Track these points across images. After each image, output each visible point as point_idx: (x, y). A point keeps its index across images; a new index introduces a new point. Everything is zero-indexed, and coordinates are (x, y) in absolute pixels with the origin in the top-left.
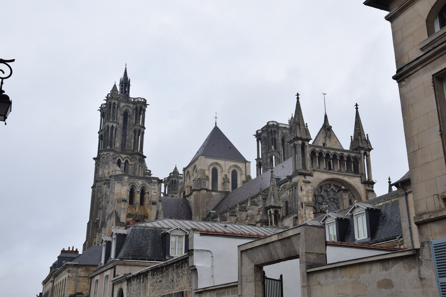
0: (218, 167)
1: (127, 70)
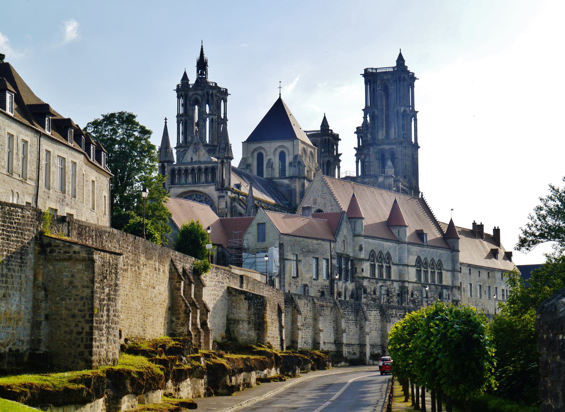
0: (263, 151)
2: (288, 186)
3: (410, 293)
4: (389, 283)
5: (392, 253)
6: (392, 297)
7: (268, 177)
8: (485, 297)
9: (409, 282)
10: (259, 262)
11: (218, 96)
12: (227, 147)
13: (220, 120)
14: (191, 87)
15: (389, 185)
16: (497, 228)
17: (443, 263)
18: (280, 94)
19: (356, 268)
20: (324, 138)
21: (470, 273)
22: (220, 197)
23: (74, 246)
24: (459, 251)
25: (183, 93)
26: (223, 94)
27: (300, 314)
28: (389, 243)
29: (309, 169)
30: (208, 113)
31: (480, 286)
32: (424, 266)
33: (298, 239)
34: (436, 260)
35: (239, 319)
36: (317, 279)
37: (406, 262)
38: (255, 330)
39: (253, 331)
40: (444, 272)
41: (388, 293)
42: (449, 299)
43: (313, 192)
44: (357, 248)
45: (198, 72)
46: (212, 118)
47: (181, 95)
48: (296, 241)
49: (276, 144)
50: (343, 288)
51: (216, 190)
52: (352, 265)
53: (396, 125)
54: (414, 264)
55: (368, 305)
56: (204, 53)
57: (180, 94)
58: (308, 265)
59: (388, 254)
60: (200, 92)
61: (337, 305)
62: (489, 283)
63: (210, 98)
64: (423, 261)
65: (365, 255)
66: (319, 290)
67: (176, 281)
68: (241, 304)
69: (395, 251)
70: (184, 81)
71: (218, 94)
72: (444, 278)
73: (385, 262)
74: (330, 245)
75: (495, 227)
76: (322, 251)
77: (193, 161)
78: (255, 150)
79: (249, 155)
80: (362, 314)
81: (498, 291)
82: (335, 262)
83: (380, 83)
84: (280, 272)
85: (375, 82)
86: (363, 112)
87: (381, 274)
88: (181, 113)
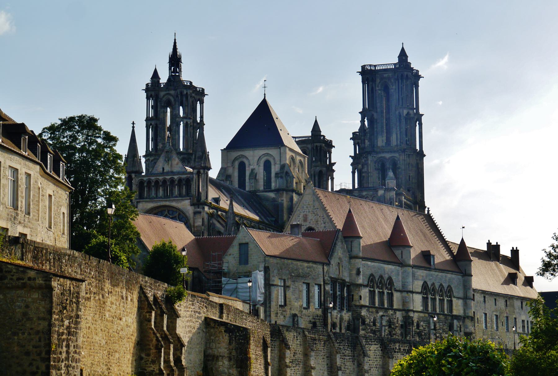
1: (177, 41)
2: (274, 200)
3: (415, 324)
4: (391, 312)
5: (394, 278)
6: (394, 329)
7: (252, 189)
8: (502, 329)
9: (414, 312)
10: (240, 289)
11: (194, 97)
12: (204, 155)
13: (195, 124)
14: (162, 86)
15: (390, 199)
16: (515, 249)
17: (453, 289)
18: (265, 95)
19: (353, 295)
20: (315, 144)
21: (485, 301)
22: (195, 213)
23: (29, 271)
24: (472, 276)
25: (153, 93)
26: (200, 94)
27: (289, 348)
28: (390, 266)
29: (298, 181)
30: (182, 116)
31: (497, 316)
32: (431, 293)
33: (286, 261)
34: (445, 285)
35: (218, 354)
36: (308, 308)
37: (410, 288)
38: (237, 367)
39: (235, 369)
40: (454, 300)
41: (390, 324)
42: (461, 331)
43: (303, 207)
44: (354, 272)
45: (170, 69)
46: (187, 122)
47: (151, 96)
48: (283, 264)
49: (260, 152)
50: (338, 318)
51: (191, 205)
52: (349, 292)
53: (398, 130)
54: (420, 290)
55: (366, 338)
56: (178, 47)
57: (149, 95)
58: (297, 292)
59: (390, 278)
60: (172, 92)
61: (331, 338)
62: (507, 313)
63: (184, 99)
64: (430, 287)
65: (363, 279)
66: (310, 321)
67: (146, 311)
68: (221, 337)
69: (398, 275)
70: (154, 80)
71: (193, 95)
72: (454, 307)
73: (387, 288)
74: (323, 268)
75: (513, 248)
76: (314, 275)
77: (165, 171)
78: (236, 159)
79: (229, 165)
80: (361, 348)
81: (517, 322)
82: (328, 288)
83: (380, 82)
84: (265, 300)
85: (374, 81)
86: (360, 114)
87: (382, 302)
88: (151, 116)
